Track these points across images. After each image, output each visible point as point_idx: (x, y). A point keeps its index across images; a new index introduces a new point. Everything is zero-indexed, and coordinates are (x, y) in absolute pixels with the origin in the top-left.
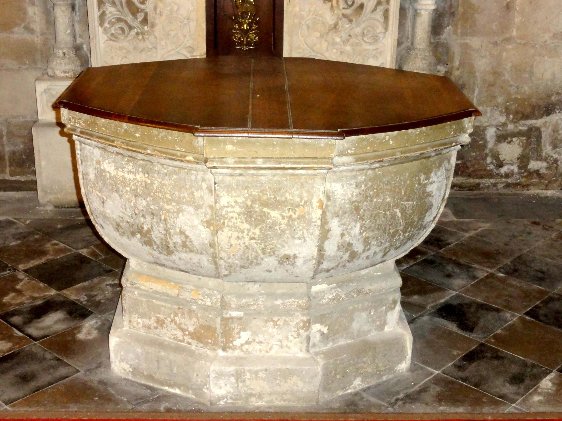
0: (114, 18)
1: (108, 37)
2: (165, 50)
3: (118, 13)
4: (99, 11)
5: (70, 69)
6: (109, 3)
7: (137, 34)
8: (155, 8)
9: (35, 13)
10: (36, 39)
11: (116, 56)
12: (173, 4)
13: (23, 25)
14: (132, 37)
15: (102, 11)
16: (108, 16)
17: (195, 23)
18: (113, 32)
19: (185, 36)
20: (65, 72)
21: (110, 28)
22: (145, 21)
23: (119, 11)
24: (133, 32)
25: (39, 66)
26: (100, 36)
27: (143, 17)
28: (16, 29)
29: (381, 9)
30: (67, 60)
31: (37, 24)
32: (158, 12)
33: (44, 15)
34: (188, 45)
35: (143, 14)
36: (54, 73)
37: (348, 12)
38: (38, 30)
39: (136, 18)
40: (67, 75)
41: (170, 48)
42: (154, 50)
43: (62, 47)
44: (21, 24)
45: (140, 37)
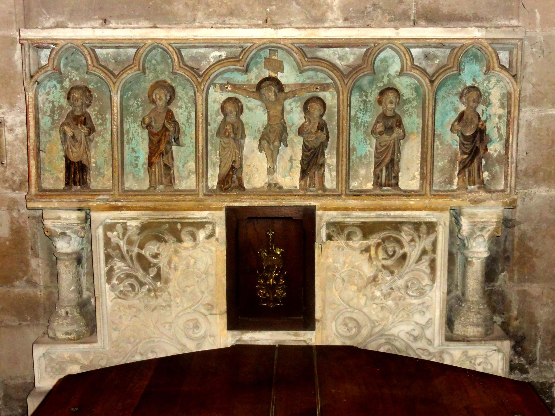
0: (122, 274)
1: (116, 294)
2: (180, 309)
3: (127, 268)
4: (106, 266)
5: (73, 330)
7: (149, 290)
8: (169, 263)
9: (38, 266)
10: (39, 293)
11: (125, 315)
12: (190, 258)
13: (25, 278)
14: (143, 294)
15: (109, 266)
17: (214, 278)
18: (122, 289)
19: (203, 293)
20: (67, 334)
21: (118, 284)
22: (158, 276)
23: (129, 267)
24: (145, 289)
25: (41, 322)
26: (107, 294)
27: (155, 273)
28: (17, 283)
29: (426, 258)
30: (69, 320)
31: (41, 277)
32: (173, 266)
33: (48, 268)
34: (207, 302)
35: (156, 270)
36: (55, 335)
37: (389, 262)
38: (42, 284)
39: (148, 274)
40: (69, 337)
41: (186, 306)
42: (168, 308)
43: (64, 305)
44: (23, 277)
45: (152, 294)
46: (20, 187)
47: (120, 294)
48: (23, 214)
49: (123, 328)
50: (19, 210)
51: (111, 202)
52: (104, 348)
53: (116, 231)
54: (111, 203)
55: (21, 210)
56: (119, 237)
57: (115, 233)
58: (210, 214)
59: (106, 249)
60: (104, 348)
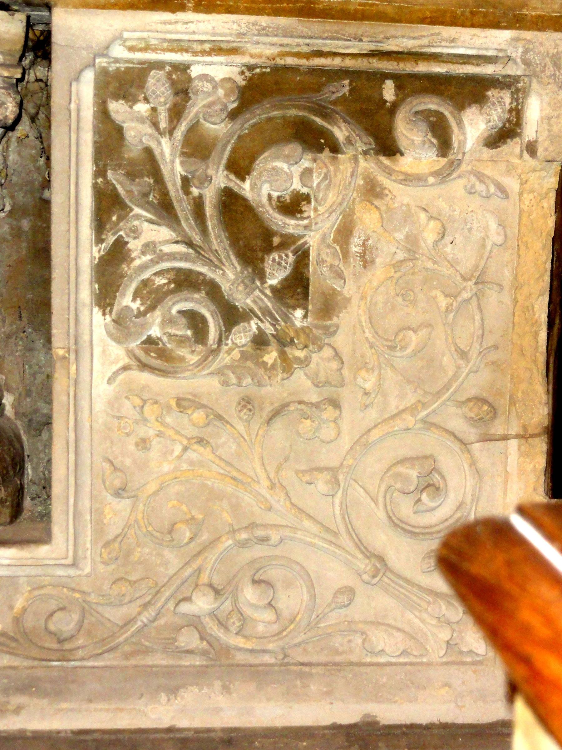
0: (157, 274)
1: (131, 353)
2: (373, 415)
3: (181, 248)
4: (99, 240)
6: (147, 205)
11: (160, 435)
12: (423, 216)
14: (236, 354)
15: (111, 239)
16: (137, 263)
17: (507, 299)
18: (155, 331)
19: (463, 355)
21: (141, 314)
23: (190, 244)
26: (97, 351)
27: (288, 272)
32: (354, 249)
34: (473, 392)
35: (291, 258)
39: (261, 275)
41: (394, 405)
42: (329, 413)
47: (147, 352)
49: (152, 487)
52: (74, 565)
53: (146, 100)
56: (155, 125)
57: (142, 108)
58: (516, 40)
59: (100, 172)
60: (74, 565)
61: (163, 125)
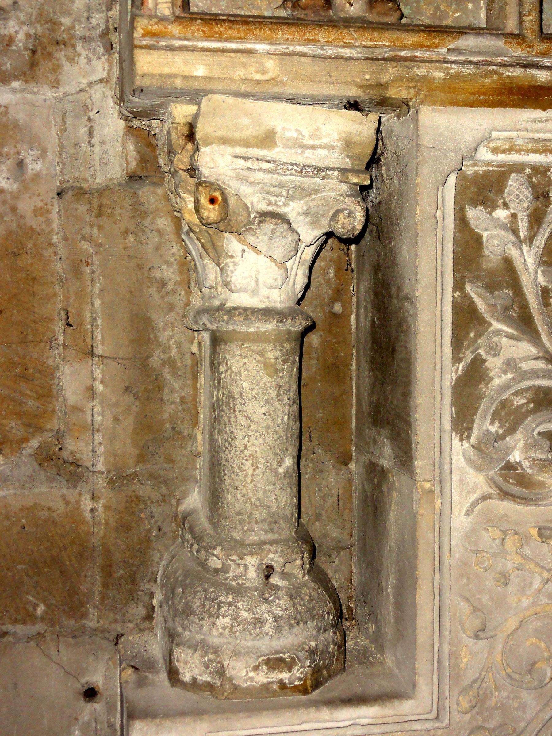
0: (516, 393)
1: (491, 481)
3: (541, 365)
5: (301, 647)
6: (506, 319)
9: (91, 392)
10: (87, 504)
13: (35, 443)
15: (469, 357)
16: (496, 382)
18: (516, 456)
25: (91, 623)
30: (284, 601)
31: (98, 437)
33: (129, 398)
36: (221, 672)
38: (100, 466)
40: (285, 676)
43: (253, 538)
44: (26, 440)
46: (33, 65)
47: (505, 478)
48: (37, 176)
49: (511, 624)
50: (21, 164)
51: (504, 65)
52: (437, 718)
53: (506, 206)
54: (507, 72)
55: (29, 160)
56: (515, 232)
57: (501, 214)
59: (458, 286)
60: (437, 718)
61: (523, 233)
